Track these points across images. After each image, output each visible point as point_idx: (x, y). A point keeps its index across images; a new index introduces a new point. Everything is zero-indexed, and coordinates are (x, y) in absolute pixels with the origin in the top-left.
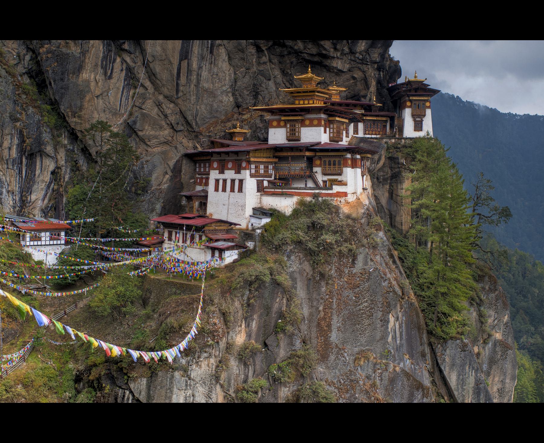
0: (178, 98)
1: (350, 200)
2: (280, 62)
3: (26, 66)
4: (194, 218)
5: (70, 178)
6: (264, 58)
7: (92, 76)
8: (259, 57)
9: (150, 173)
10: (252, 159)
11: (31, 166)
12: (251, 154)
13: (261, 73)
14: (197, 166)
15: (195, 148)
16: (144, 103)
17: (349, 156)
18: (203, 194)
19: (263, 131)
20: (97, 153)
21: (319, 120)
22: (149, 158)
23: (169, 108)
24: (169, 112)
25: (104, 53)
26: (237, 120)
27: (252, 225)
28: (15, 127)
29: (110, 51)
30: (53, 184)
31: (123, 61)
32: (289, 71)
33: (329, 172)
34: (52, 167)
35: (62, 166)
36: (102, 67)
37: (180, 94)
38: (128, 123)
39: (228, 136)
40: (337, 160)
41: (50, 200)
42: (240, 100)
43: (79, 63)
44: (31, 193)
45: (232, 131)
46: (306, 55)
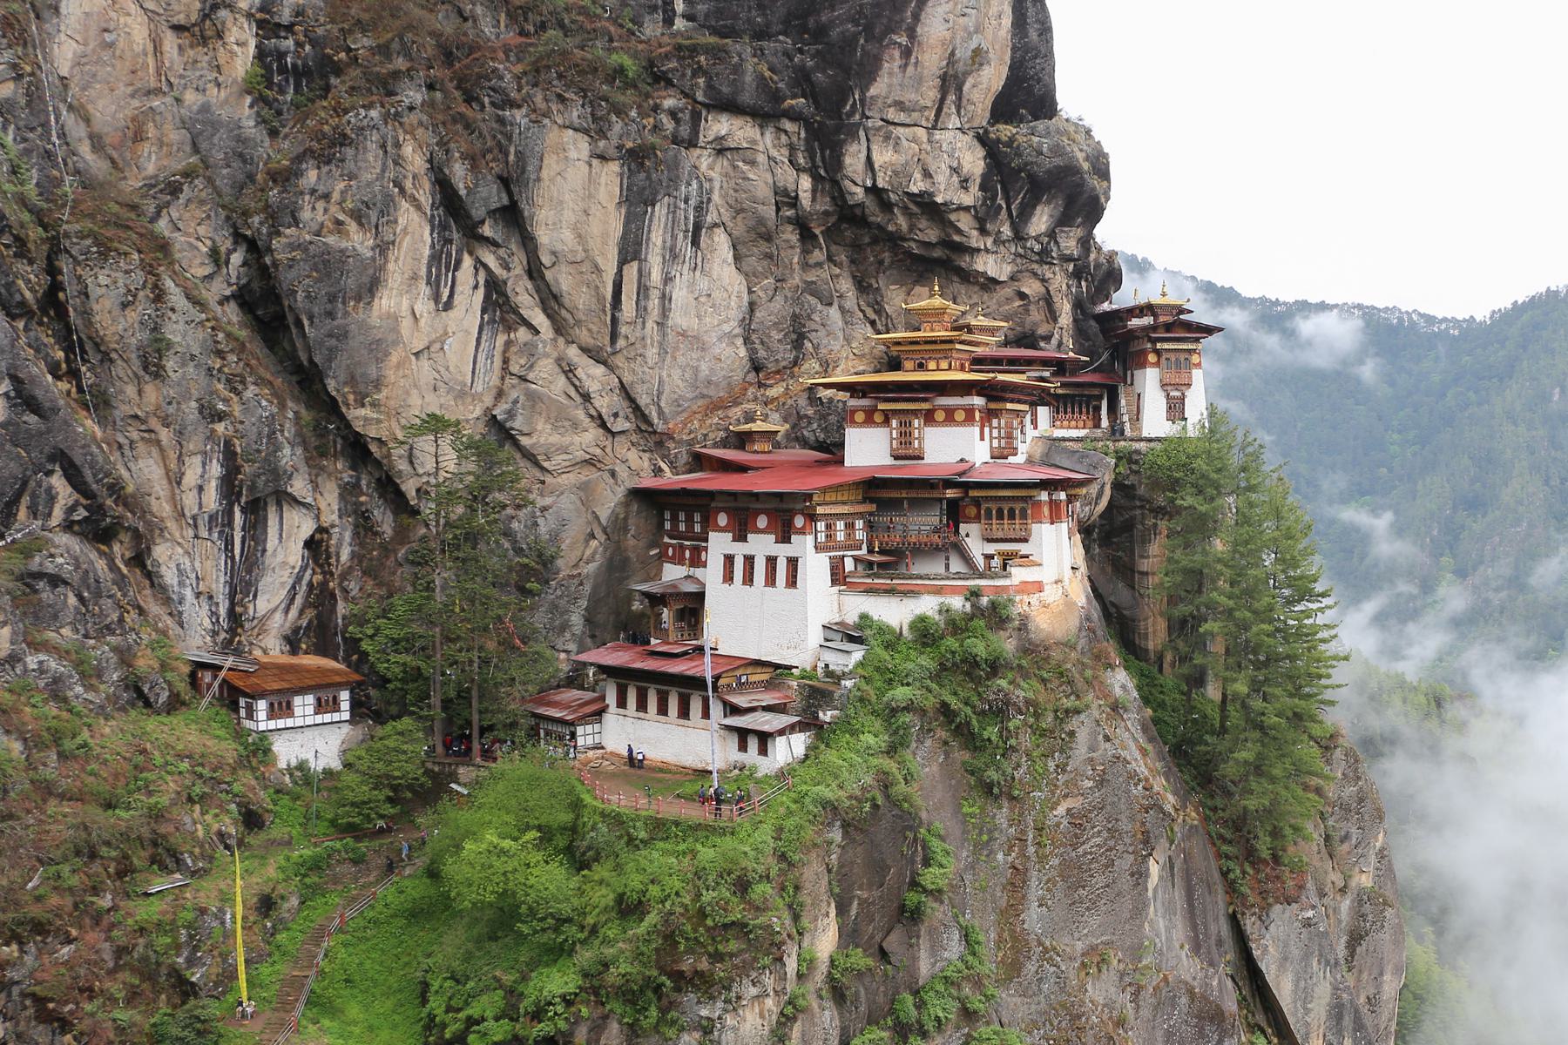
0: (614, 353)
1: (1050, 600)
2: (853, 262)
3: (233, 280)
4: (685, 653)
5: (353, 555)
6: (817, 252)
7: (405, 304)
8: (806, 252)
9: (555, 537)
10: (820, 510)
11: (256, 529)
12: (815, 498)
13: (811, 288)
14: (667, 515)
15: (658, 471)
16: (532, 366)
17: (1044, 496)
18: (690, 588)
19: (815, 426)
20: (418, 491)
21: (970, 412)
22: (548, 501)
23: (593, 375)
24: (592, 387)
25: (433, 246)
26: (755, 399)
27: (827, 666)
28: (212, 436)
29: (451, 241)
30: (309, 572)
31: (480, 264)
32: (873, 281)
33: (1000, 535)
34: (307, 528)
35: (333, 526)
36: (428, 283)
37: (621, 343)
38: (494, 417)
39: (733, 440)
40: (1018, 507)
41: (301, 612)
42: (762, 353)
43: (371, 271)
44: (255, 596)
45: (746, 427)
46: (913, 245)
